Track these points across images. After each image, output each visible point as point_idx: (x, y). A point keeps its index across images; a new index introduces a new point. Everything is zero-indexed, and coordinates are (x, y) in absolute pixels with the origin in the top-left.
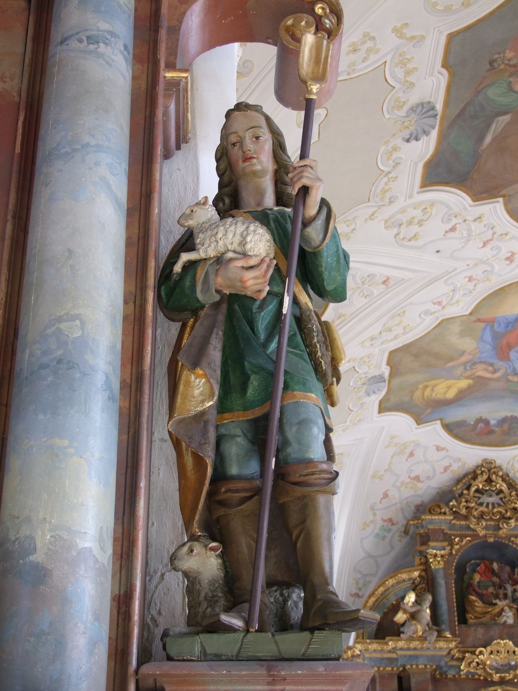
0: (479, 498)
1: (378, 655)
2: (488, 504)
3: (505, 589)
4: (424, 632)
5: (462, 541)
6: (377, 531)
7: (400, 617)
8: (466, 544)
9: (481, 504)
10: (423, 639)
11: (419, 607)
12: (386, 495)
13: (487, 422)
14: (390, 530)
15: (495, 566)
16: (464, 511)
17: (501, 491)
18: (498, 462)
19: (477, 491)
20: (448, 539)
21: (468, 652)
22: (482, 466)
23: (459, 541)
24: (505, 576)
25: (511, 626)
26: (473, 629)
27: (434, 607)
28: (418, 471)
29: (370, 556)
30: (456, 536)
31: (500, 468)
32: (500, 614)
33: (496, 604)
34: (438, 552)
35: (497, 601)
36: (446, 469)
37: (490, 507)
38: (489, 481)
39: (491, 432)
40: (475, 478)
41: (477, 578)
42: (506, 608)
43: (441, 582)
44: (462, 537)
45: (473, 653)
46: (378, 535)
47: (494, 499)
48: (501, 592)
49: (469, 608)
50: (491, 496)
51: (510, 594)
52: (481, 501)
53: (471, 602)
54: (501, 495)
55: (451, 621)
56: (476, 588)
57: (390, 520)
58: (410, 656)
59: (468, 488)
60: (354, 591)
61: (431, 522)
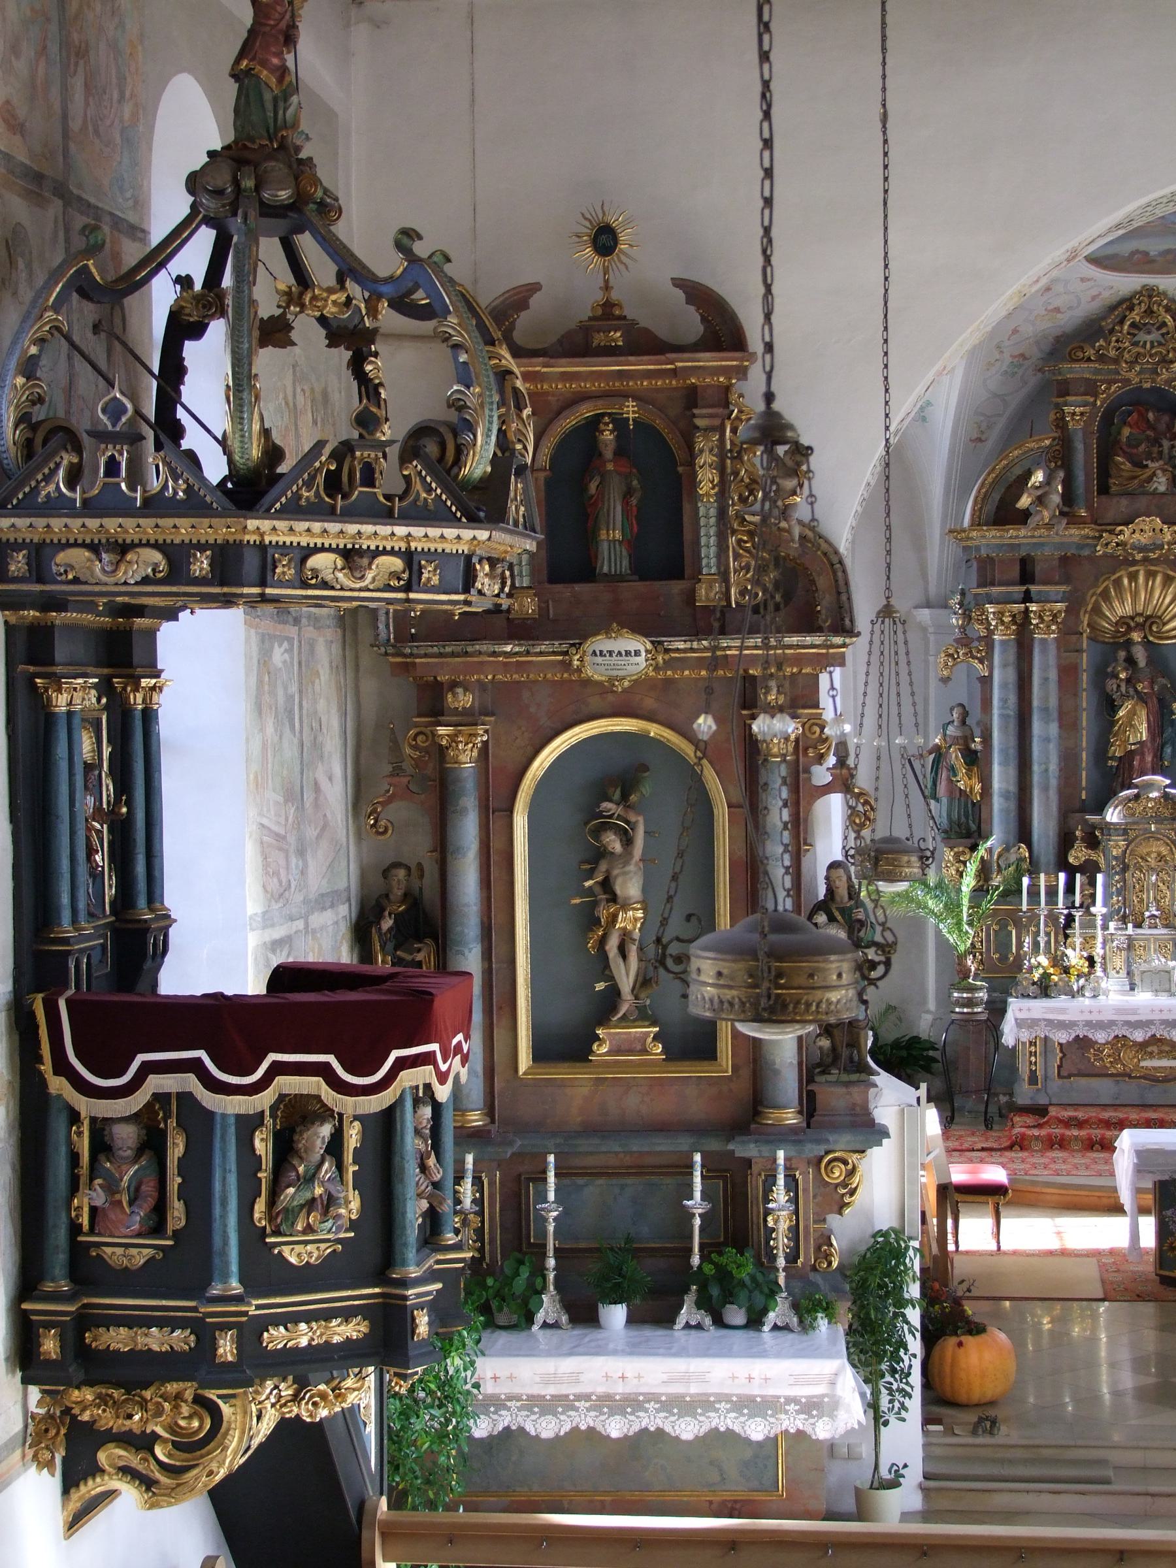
0: (1134, 335)
1: (998, 541)
2: (1145, 343)
3: (1161, 446)
4: (1053, 517)
5: (1108, 388)
6: (1004, 368)
7: (1025, 502)
8: (1115, 392)
9: (1136, 344)
10: (1049, 526)
11: (1047, 488)
12: (1015, 331)
13: (1146, 254)
14: (1021, 365)
15: (1151, 416)
16: (1112, 353)
17: (1164, 324)
18: (1161, 288)
19: (1133, 325)
20: (1091, 388)
21: (1106, 531)
22: (1140, 293)
23: (1106, 388)
24: (1162, 427)
25: (1163, 494)
26: (1115, 500)
27: (1068, 483)
28: (1057, 303)
29: (996, 395)
30: (1103, 382)
31: (1165, 294)
32: (1150, 480)
33: (1146, 466)
34: (1077, 410)
35: (1149, 462)
36: (1094, 298)
37: (1148, 346)
38: (1149, 312)
39: (1152, 261)
40: (1131, 309)
41: (1126, 431)
42: (1159, 472)
43: (1079, 446)
44: (1110, 383)
45: (1111, 532)
46: (1006, 372)
47: (1155, 336)
48: (1155, 449)
49: (1113, 472)
50: (1149, 333)
51: (1166, 451)
52: (1136, 339)
53: (1117, 464)
54: (1164, 330)
55: (1088, 490)
56: (1124, 447)
57: (1022, 355)
58: (1035, 544)
59: (1121, 322)
60: (975, 436)
61: (1071, 370)
